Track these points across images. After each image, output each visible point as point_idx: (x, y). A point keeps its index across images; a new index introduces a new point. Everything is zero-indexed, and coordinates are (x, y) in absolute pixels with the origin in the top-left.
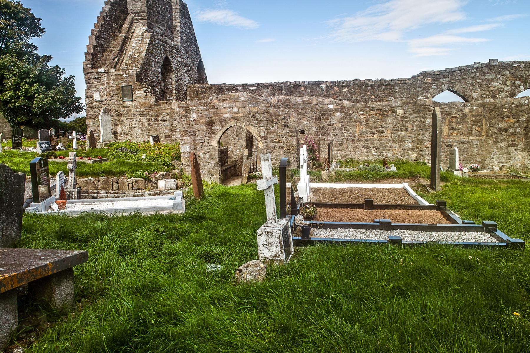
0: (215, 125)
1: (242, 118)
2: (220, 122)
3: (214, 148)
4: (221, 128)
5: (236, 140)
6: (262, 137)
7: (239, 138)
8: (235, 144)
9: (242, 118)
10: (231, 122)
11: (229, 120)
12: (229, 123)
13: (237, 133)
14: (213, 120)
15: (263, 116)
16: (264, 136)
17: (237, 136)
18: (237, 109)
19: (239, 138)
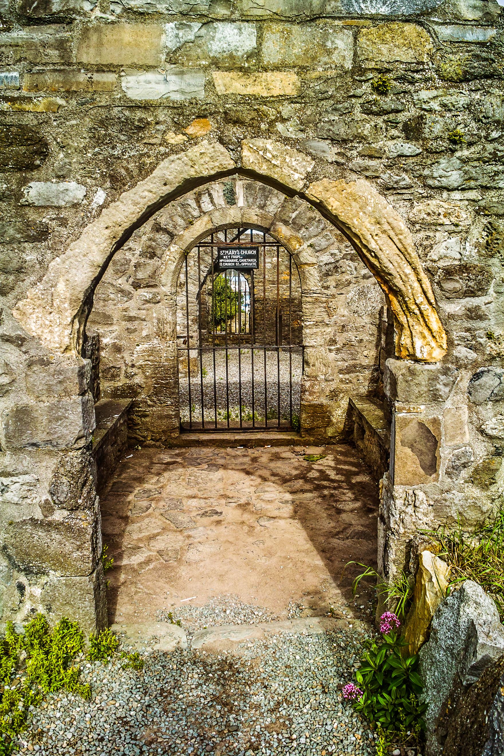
0: (47, 170)
1: (286, 109)
2: (98, 141)
3: (45, 363)
4: (100, 196)
5: (132, 304)
6: (449, 273)
7: (149, 296)
8: (131, 319)
9: (286, 109)
10: (193, 141)
11: (179, 127)
12: (175, 150)
13: (140, 275)
14: (29, 120)
15: (463, 100)
16: (464, 268)
17: (137, 286)
18: (250, 29)
19: (145, 293)
